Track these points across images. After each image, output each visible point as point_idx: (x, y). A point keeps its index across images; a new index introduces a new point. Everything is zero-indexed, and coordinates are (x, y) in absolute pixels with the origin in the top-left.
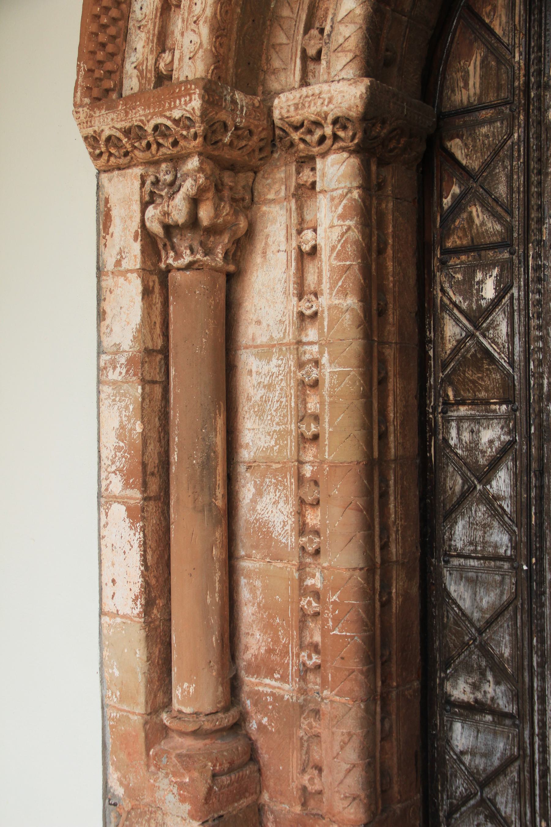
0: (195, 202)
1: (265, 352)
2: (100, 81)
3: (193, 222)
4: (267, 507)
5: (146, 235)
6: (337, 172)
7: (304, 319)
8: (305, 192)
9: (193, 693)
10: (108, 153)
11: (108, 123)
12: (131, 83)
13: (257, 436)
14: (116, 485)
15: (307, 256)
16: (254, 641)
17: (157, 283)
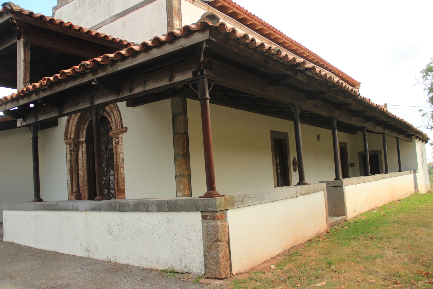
0: (73, 148)
1: (80, 160)
2: (66, 138)
3: (73, 149)
4: (81, 173)
5: (70, 150)
6: (84, 145)
7: (83, 157)
8: (82, 146)
9: (75, 189)
10: (67, 143)
11: (66, 141)
12: (69, 138)
13: (80, 167)
14: (68, 172)
15: (83, 152)
16: (80, 185)
17: (71, 154)
